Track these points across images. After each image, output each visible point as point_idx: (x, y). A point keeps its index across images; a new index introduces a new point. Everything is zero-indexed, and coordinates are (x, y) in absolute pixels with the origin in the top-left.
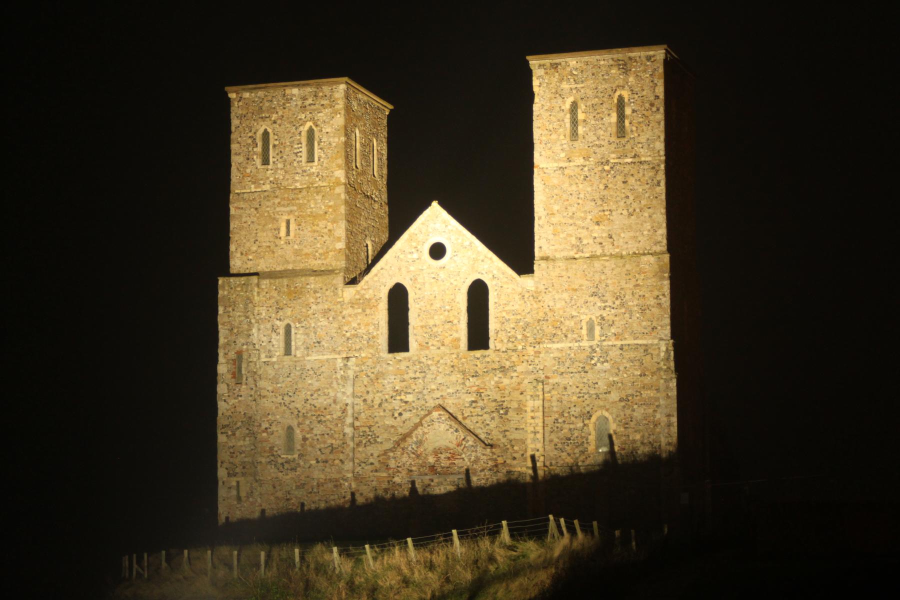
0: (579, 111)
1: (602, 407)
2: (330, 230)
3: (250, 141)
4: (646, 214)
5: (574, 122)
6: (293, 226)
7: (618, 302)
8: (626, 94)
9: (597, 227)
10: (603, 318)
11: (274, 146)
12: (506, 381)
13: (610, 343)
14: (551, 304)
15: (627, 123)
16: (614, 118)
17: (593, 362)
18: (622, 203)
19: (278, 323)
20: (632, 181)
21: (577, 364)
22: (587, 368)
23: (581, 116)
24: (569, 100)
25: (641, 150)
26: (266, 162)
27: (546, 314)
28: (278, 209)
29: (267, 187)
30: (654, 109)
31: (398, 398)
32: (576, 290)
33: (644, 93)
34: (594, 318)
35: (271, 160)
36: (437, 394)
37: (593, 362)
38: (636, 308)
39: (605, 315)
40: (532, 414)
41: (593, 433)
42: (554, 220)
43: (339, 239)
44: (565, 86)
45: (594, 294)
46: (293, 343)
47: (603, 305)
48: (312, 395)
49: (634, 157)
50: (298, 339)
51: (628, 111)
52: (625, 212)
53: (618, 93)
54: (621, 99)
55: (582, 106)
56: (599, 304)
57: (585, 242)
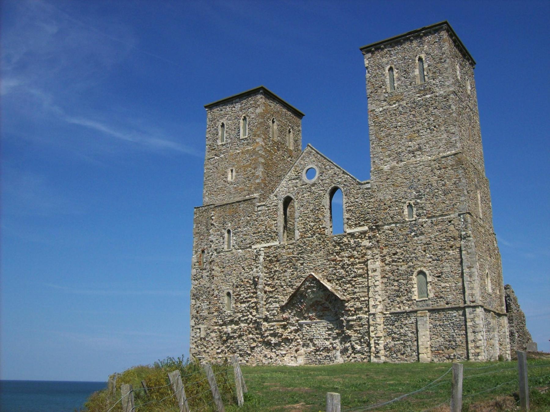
0: (394, 73)
1: (420, 267)
2: (253, 173)
3: (215, 132)
4: (443, 128)
5: (392, 80)
6: (234, 173)
7: (428, 190)
8: (423, 56)
9: (410, 143)
10: (418, 203)
11: (227, 131)
12: (355, 253)
13: (424, 220)
14: (382, 198)
15: (425, 73)
16: (417, 72)
17: (413, 234)
18: (426, 124)
19: (223, 231)
20: (431, 109)
21: (401, 237)
22: (408, 239)
23: (396, 75)
24: (387, 68)
25: (436, 88)
26: (222, 141)
27: (379, 205)
28: (227, 165)
29: (222, 156)
30: (443, 61)
31: (288, 271)
32: (398, 186)
33: (436, 52)
34: (412, 202)
35: (225, 139)
36: (312, 266)
37: (413, 234)
38: (440, 192)
39: (418, 201)
40: (372, 274)
41: (415, 286)
42: (382, 143)
43: (257, 177)
44: (384, 60)
45: (410, 187)
46: (231, 242)
47: (417, 194)
48: (240, 273)
49: (432, 93)
51: (426, 66)
52: (429, 131)
53: (418, 56)
54: (420, 59)
55: (395, 71)
56: (414, 193)
57: (402, 155)
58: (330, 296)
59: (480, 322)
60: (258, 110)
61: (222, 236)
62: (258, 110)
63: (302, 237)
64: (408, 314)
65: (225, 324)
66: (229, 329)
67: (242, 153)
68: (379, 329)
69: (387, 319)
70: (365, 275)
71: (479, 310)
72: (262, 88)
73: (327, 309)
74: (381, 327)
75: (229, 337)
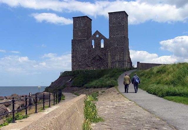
50: (81, 47)
58: (101, 58)
59: (126, 64)
60: (85, 21)
61: (78, 46)
62: (85, 21)
63: (95, 47)
64: (115, 62)
65: (79, 62)
66: (80, 64)
67: (82, 29)
68: (110, 64)
69: (111, 63)
70: (107, 55)
71: (126, 62)
72: (86, 16)
73: (100, 60)
74: (110, 64)
75: (80, 65)
